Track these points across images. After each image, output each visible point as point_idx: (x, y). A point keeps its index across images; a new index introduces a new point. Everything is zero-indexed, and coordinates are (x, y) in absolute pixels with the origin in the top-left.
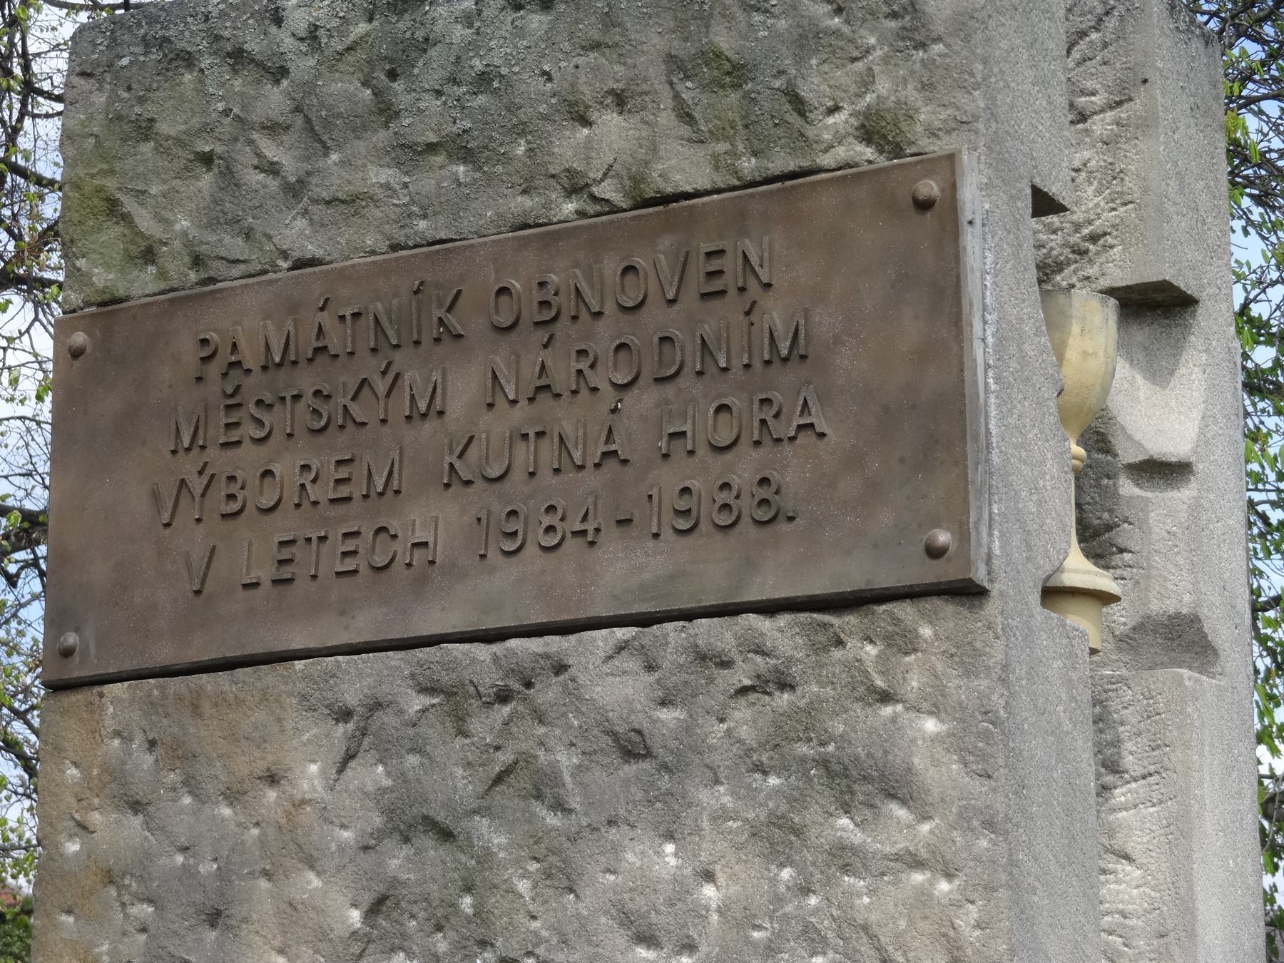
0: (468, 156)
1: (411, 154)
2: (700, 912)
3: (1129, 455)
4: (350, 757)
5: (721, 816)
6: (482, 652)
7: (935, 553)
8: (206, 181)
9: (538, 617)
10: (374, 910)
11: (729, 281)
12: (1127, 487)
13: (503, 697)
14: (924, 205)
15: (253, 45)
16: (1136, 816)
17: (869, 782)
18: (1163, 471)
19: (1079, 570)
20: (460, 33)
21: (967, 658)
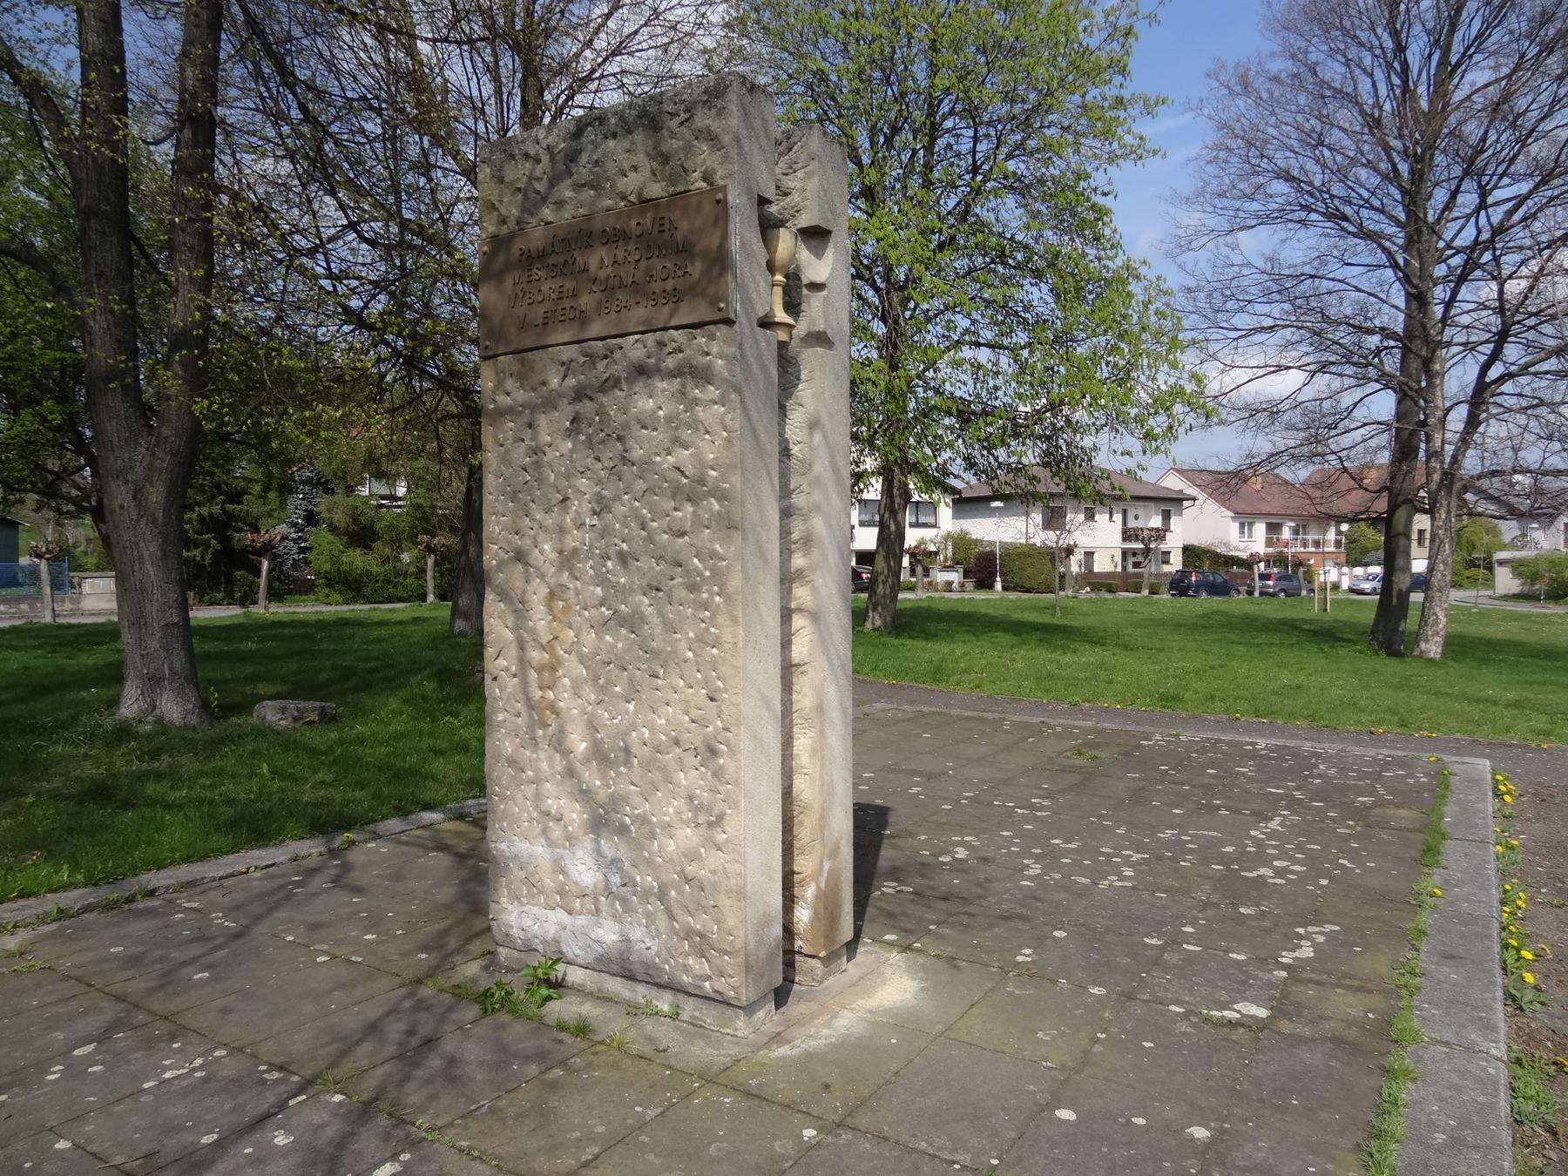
0: (593, 188)
1: (578, 187)
2: (658, 419)
3: (805, 282)
4: (565, 376)
5: (664, 390)
6: (600, 343)
7: (720, 310)
8: (520, 196)
9: (614, 333)
10: (572, 423)
11: (667, 226)
12: (805, 291)
13: (606, 357)
14: (718, 202)
15: (532, 152)
16: (804, 391)
17: (703, 376)
18: (816, 287)
19: (781, 316)
20: (590, 147)
21: (728, 342)
